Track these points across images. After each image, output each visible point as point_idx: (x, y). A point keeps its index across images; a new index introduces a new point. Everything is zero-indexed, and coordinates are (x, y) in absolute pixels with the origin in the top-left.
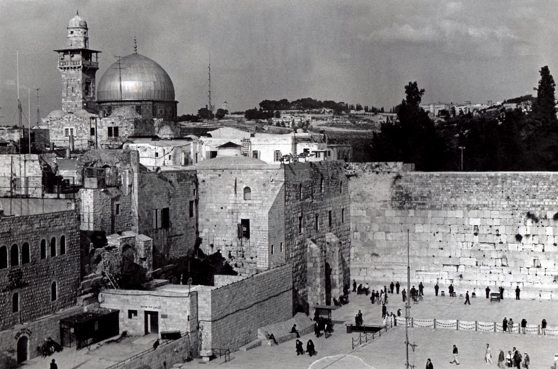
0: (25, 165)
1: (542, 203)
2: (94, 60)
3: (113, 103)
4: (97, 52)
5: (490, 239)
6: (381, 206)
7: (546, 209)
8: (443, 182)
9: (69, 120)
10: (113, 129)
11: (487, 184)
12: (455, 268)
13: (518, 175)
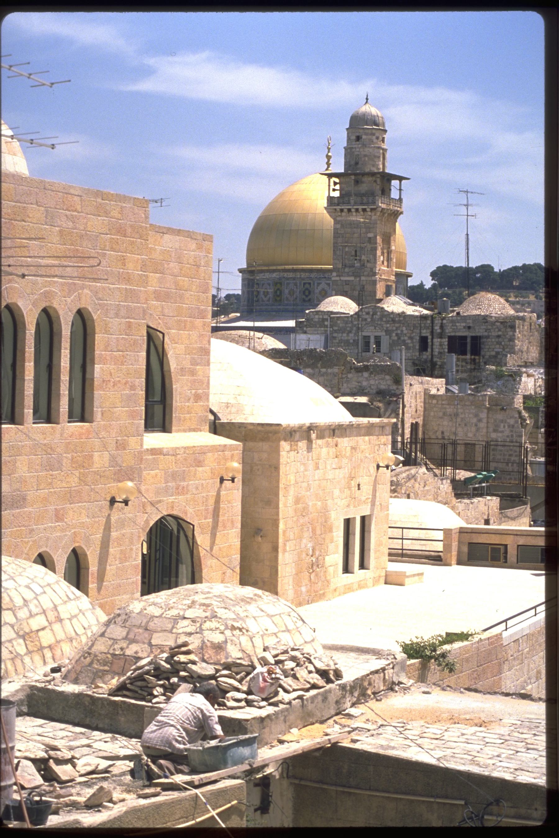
0: (488, 418)
2: (395, 194)
3: (285, 275)
4: (400, 179)
9: (372, 318)
10: (469, 340)
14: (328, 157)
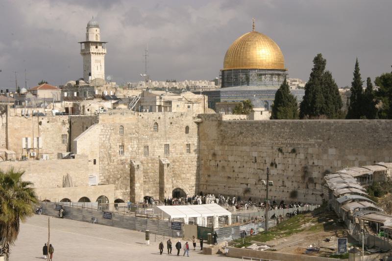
1: (286, 142)
5: (262, 167)
6: (213, 143)
7: (288, 146)
8: (240, 127)
11: (260, 128)
12: (246, 186)
13: (275, 122)
14: (253, 26)
